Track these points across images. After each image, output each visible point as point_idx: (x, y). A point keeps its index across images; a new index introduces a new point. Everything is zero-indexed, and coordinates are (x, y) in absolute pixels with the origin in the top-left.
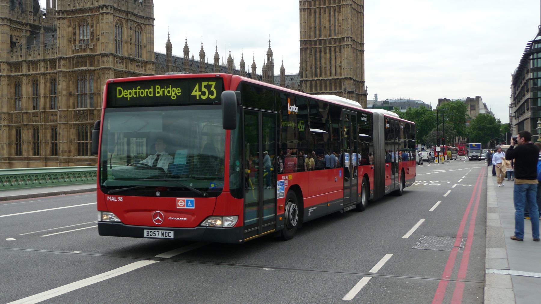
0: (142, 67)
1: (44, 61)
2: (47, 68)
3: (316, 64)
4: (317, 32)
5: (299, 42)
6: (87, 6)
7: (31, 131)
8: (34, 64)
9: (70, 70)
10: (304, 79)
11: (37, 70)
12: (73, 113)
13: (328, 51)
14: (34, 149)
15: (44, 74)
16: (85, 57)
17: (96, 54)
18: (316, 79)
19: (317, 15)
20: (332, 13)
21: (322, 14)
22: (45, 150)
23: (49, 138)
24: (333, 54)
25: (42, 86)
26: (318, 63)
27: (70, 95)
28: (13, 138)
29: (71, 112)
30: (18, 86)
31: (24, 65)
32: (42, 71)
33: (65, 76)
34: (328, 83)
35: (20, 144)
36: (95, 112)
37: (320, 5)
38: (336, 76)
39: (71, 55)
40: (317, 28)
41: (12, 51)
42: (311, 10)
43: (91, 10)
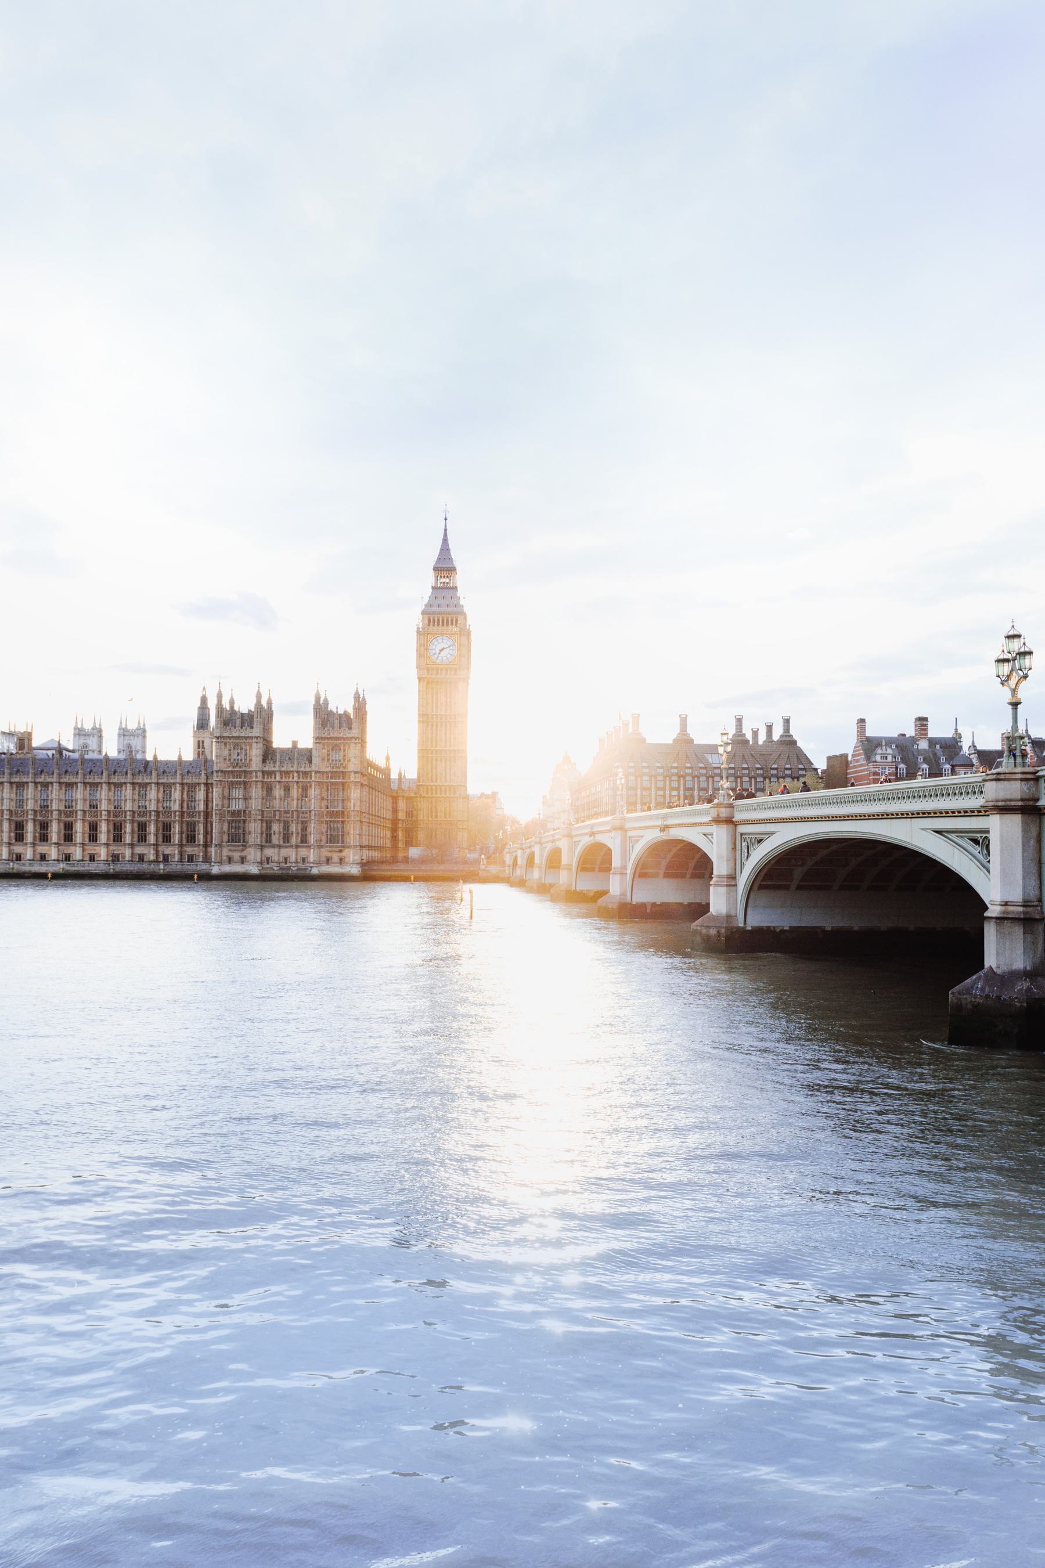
1: (298, 772)
2: (299, 778)
4: (434, 743)
7: (282, 825)
8: (287, 773)
11: (289, 778)
12: (325, 813)
14: (284, 838)
15: (298, 782)
16: (339, 772)
19: (434, 728)
20: (448, 727)
22: (294, 840)
23: (299, 830)
29: (323, 812)
30: (269, 789)
31: (278, 774)
32: (296, 779)
33: (319, 785)
34: (443, 788)
35: (270, 835)
36: (345, 813)
39: (323, 769)
42: (428, 722)
43: (344, 739)
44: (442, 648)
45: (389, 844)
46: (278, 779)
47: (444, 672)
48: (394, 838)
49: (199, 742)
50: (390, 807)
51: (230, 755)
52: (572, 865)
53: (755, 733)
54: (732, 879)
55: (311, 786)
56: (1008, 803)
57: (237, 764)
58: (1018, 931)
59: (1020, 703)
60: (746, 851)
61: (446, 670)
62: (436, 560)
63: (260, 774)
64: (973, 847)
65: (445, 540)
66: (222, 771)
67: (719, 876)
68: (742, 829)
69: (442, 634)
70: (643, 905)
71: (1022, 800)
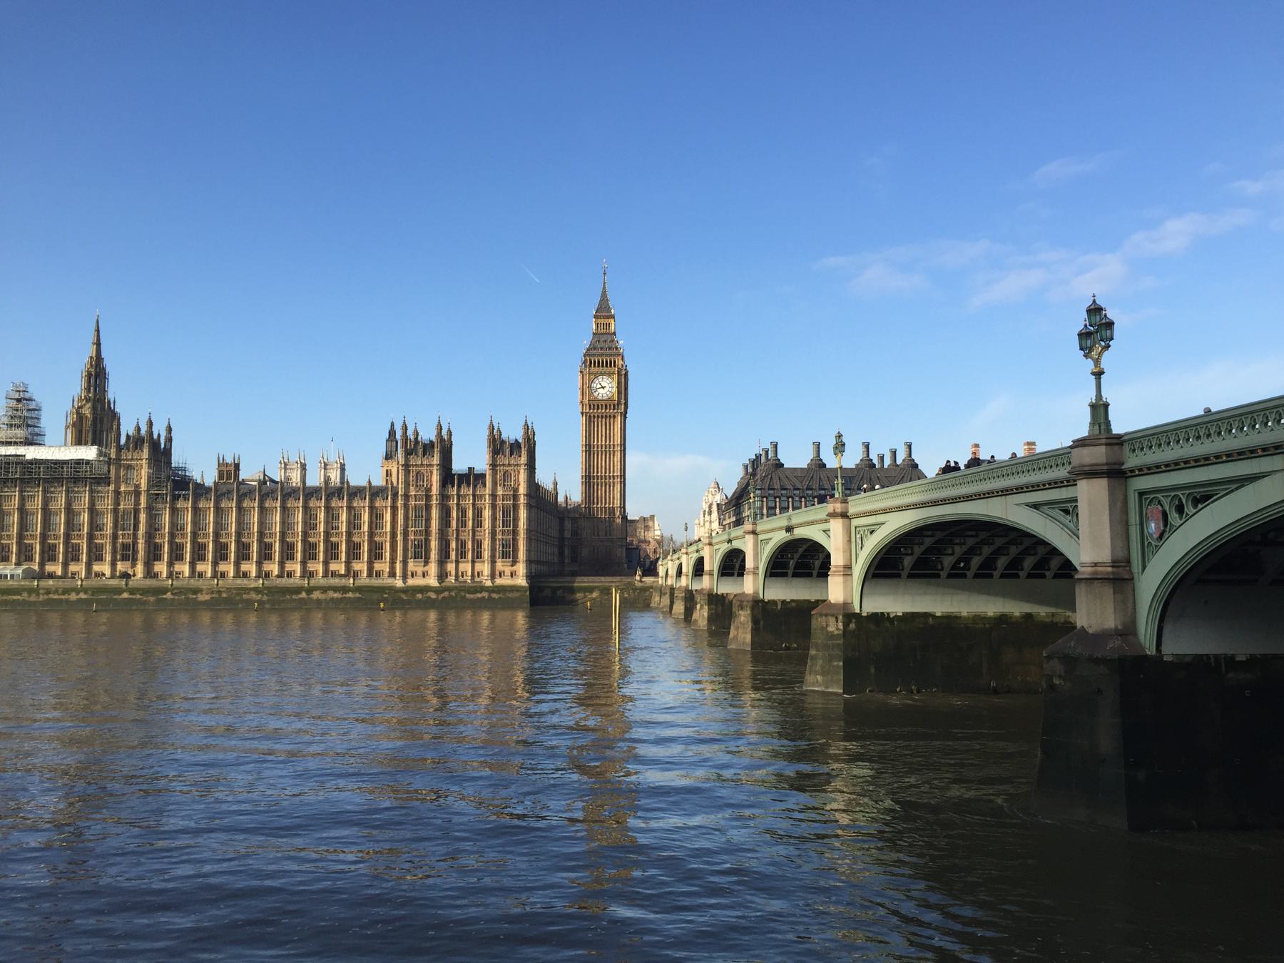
5: (580, 477)
28: (444, 547)
44: (605, 387)
45: (556, 560)
48: (561, 554)
49: (387, 471)
52: (713, 571)
53: (882, 458)
54: (848, 568)
55: (485, 508)
56: (1094, 468)
57: (419, 489)
58: (1108, 590)
59: (1103, 373)
60: (860, 542)
64: (1063, 516)
65: (604, 288)
67: (836, 566)
68: (855, 522)
69: (602, 374)
70: (774, 602)
71: (1107, 464)
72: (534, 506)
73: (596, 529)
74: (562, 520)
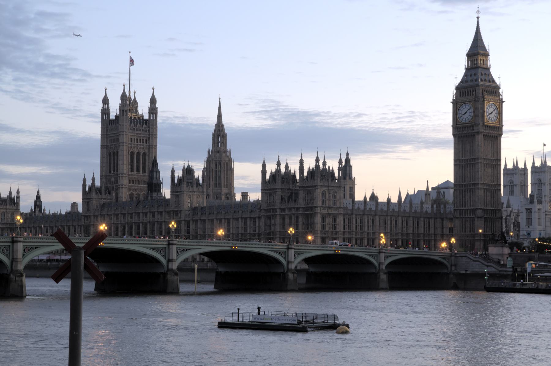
0: (336, 210)
1: (294, 208)
3: (463, 199)
4: (464, 178)
6: (310, 185)
8: (290, 209)
9: (303, 213)
10: (456, 208)
13: (469, 191)
15: (294, 214)
17: (313, 206)
18: (463, 208)
19: (464, 169)
20: (471, 167)
21: (466, 168)
24: (471, 193)
25: (293, 219)
26: (464, 198)
27: (304, 224)
30: (284, 219)
31: (286, 209)
32: (293, 212)
37: (465, 162)
38: (473, 207)
40: (464, 176)
41: (282, 203)
43: (311, 187)
46: (286, 212)
47: (466, 129)
50: (439, 225)
51: (268, 199)
61: (468, 127)
62: (468, 49)
63: (278, 211)
66: (264, 209)
69: (465, 102)
72: (341, 214)
73: (464, 226)
74: (442, 219)
